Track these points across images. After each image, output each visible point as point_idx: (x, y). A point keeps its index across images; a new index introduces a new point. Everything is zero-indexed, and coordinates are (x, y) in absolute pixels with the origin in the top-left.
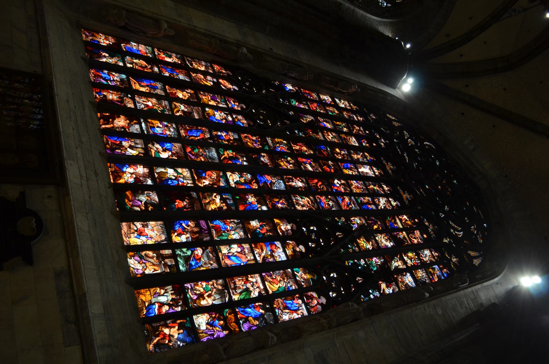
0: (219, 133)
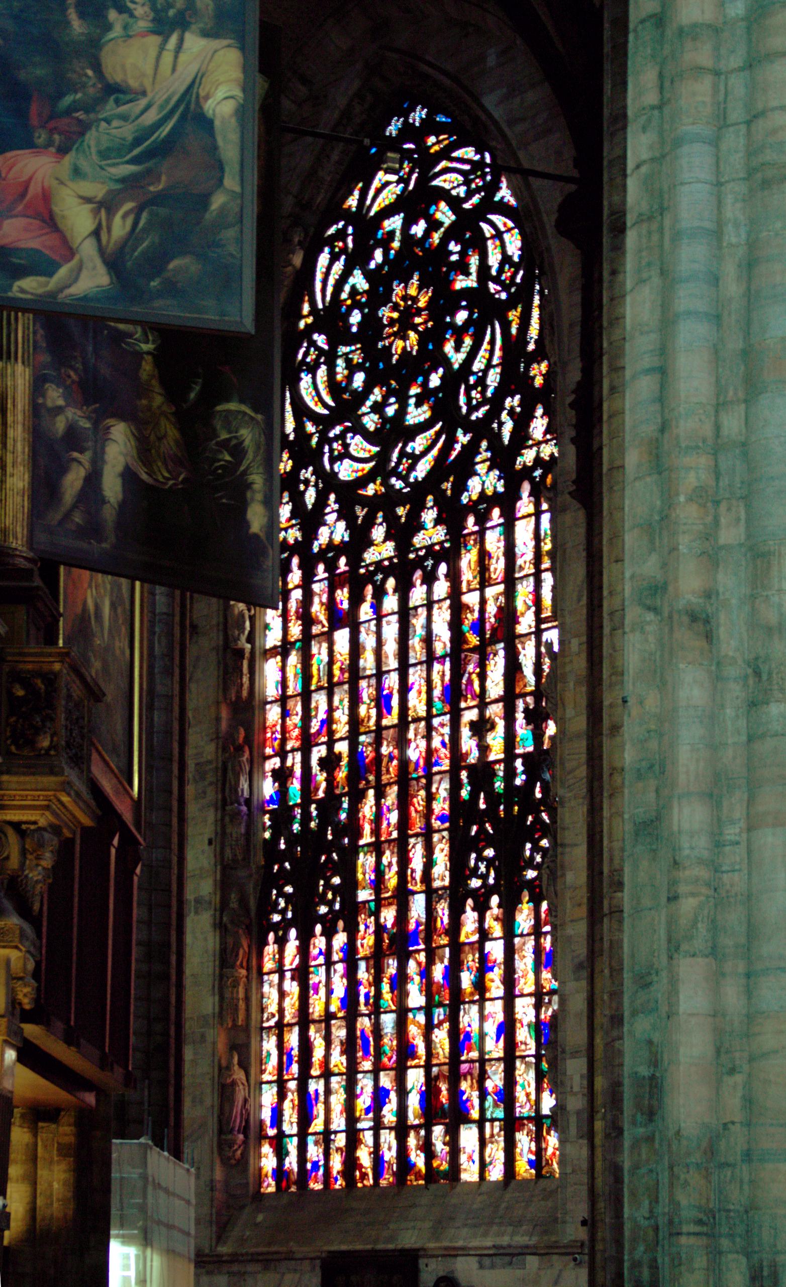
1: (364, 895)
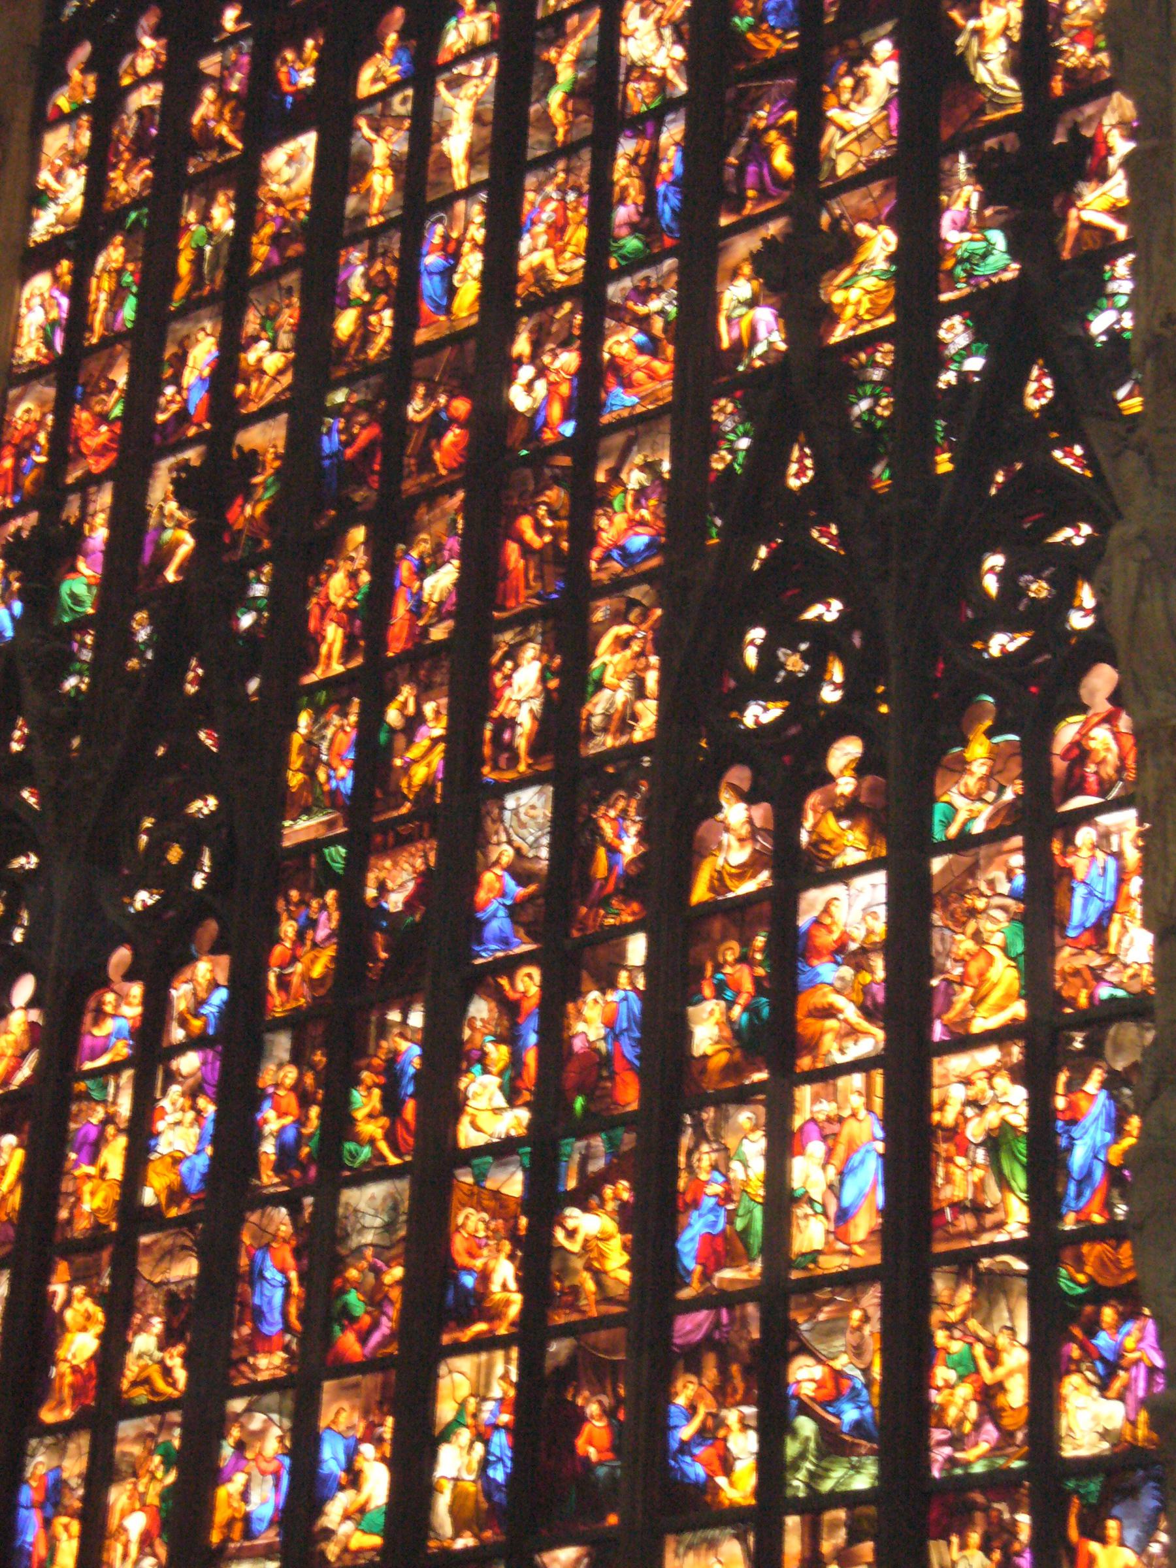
0: (269, 1148)
1: (300, 829)
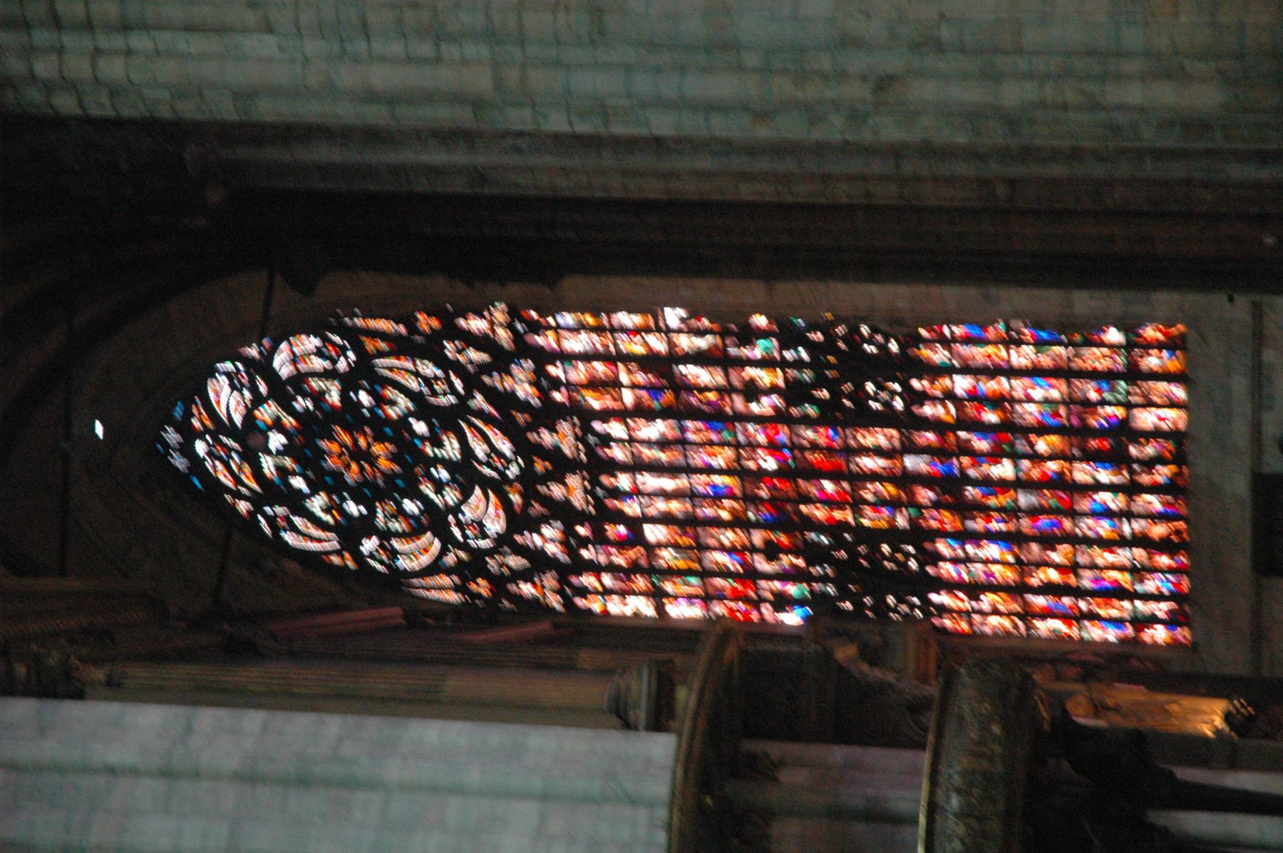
1: (901, 522)
